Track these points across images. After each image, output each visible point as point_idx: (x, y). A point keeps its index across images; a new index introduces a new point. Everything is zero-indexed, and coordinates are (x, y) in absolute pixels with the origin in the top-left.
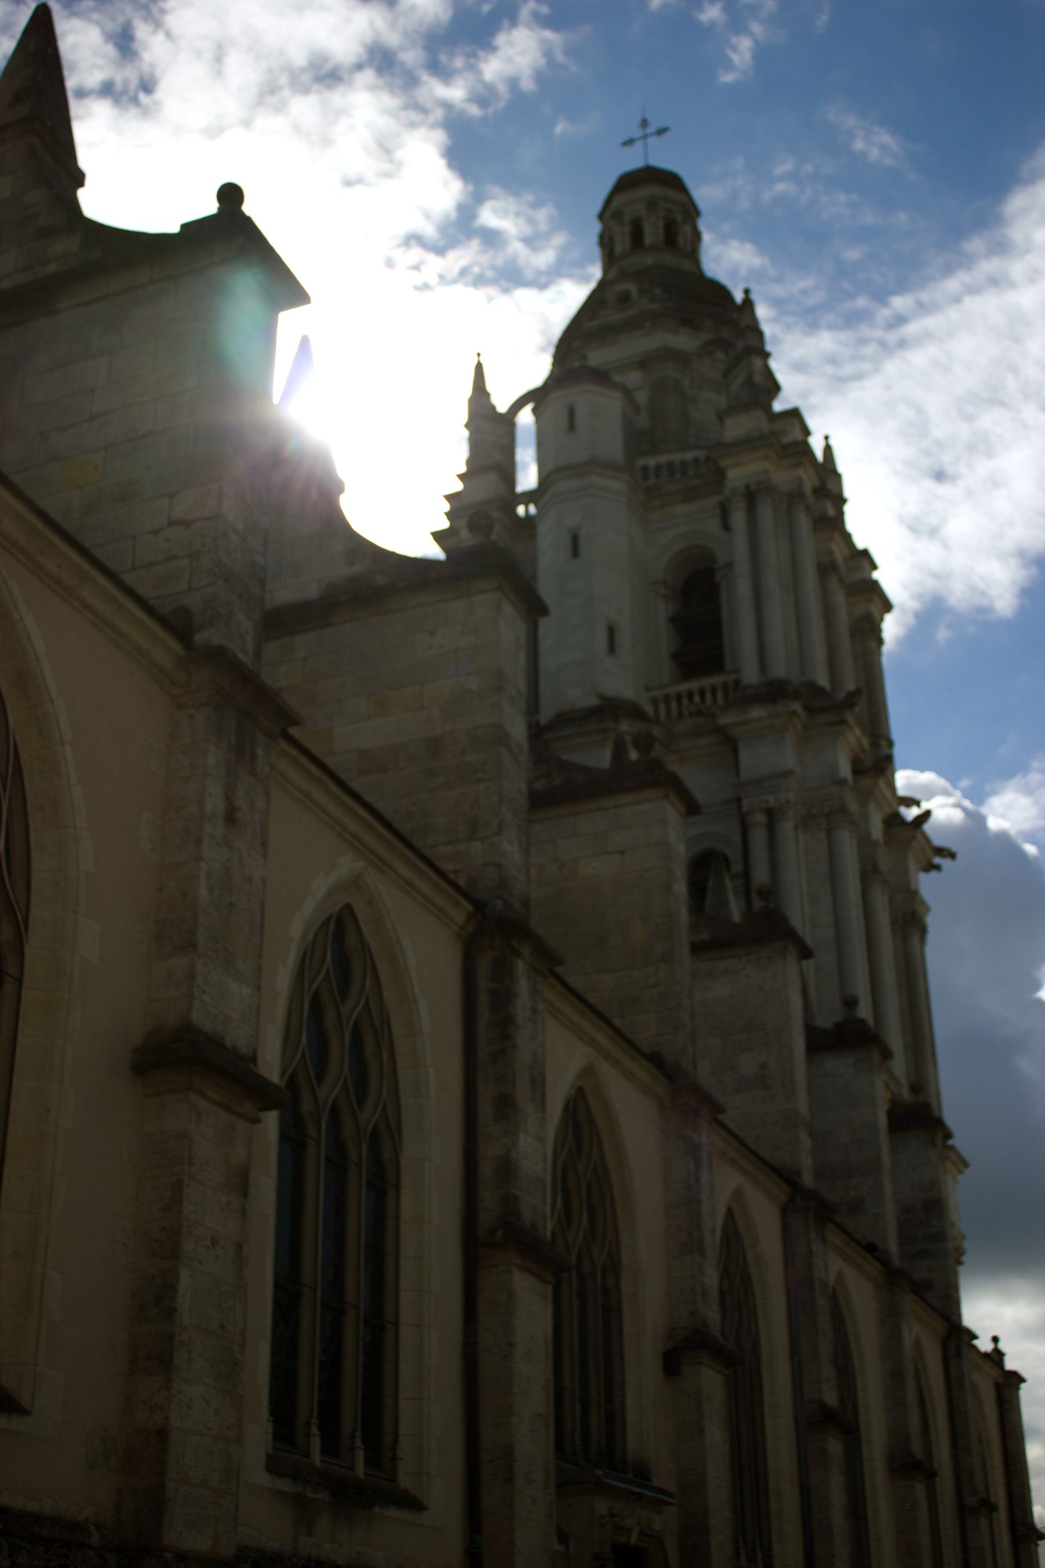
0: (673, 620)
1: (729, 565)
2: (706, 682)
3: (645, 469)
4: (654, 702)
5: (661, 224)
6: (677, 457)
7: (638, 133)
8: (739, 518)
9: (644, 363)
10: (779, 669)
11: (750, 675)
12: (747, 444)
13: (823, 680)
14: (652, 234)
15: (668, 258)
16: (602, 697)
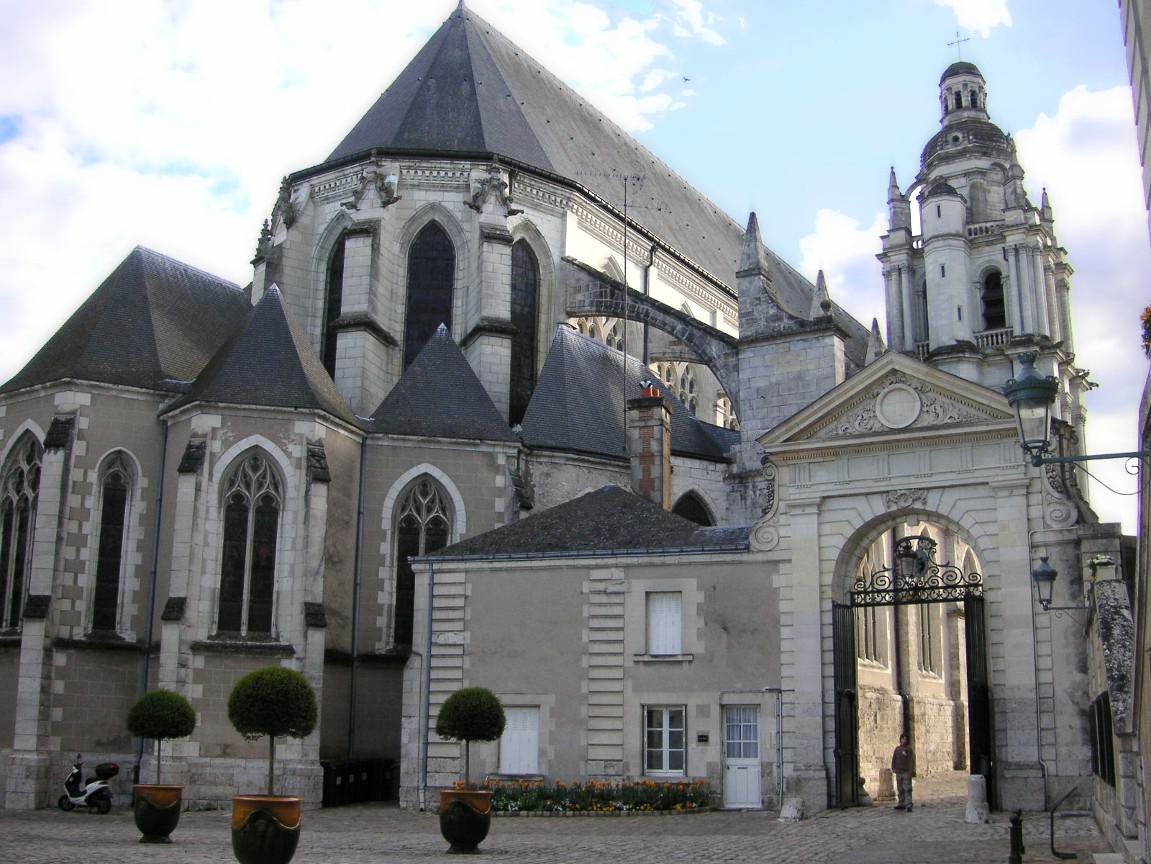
0: (983, 298)
1: (1008, 277)
2: (999, 331)
3: (970, 230)
4: (977, 338)
5: (969, 95)
6: (983, 225)
7: (955, 39)
8: (1012, 259)
9: (966, 174)
10: (1029, 330)
11: (1017, 331)
12: (1016, 226)
13: (1047, 334)
14: (966, 101)
15: (973, 114)
16: (958, 341)
